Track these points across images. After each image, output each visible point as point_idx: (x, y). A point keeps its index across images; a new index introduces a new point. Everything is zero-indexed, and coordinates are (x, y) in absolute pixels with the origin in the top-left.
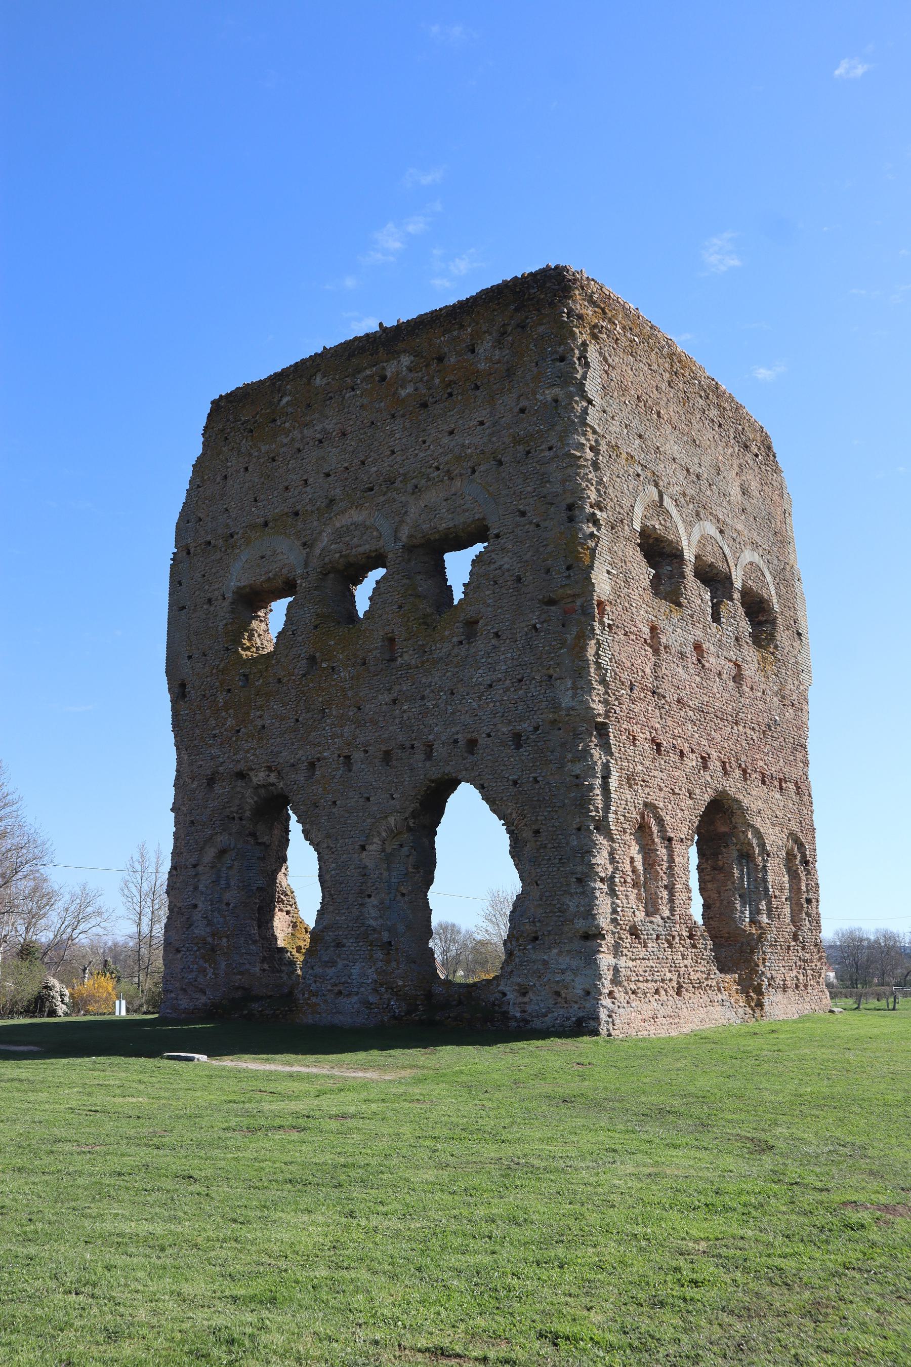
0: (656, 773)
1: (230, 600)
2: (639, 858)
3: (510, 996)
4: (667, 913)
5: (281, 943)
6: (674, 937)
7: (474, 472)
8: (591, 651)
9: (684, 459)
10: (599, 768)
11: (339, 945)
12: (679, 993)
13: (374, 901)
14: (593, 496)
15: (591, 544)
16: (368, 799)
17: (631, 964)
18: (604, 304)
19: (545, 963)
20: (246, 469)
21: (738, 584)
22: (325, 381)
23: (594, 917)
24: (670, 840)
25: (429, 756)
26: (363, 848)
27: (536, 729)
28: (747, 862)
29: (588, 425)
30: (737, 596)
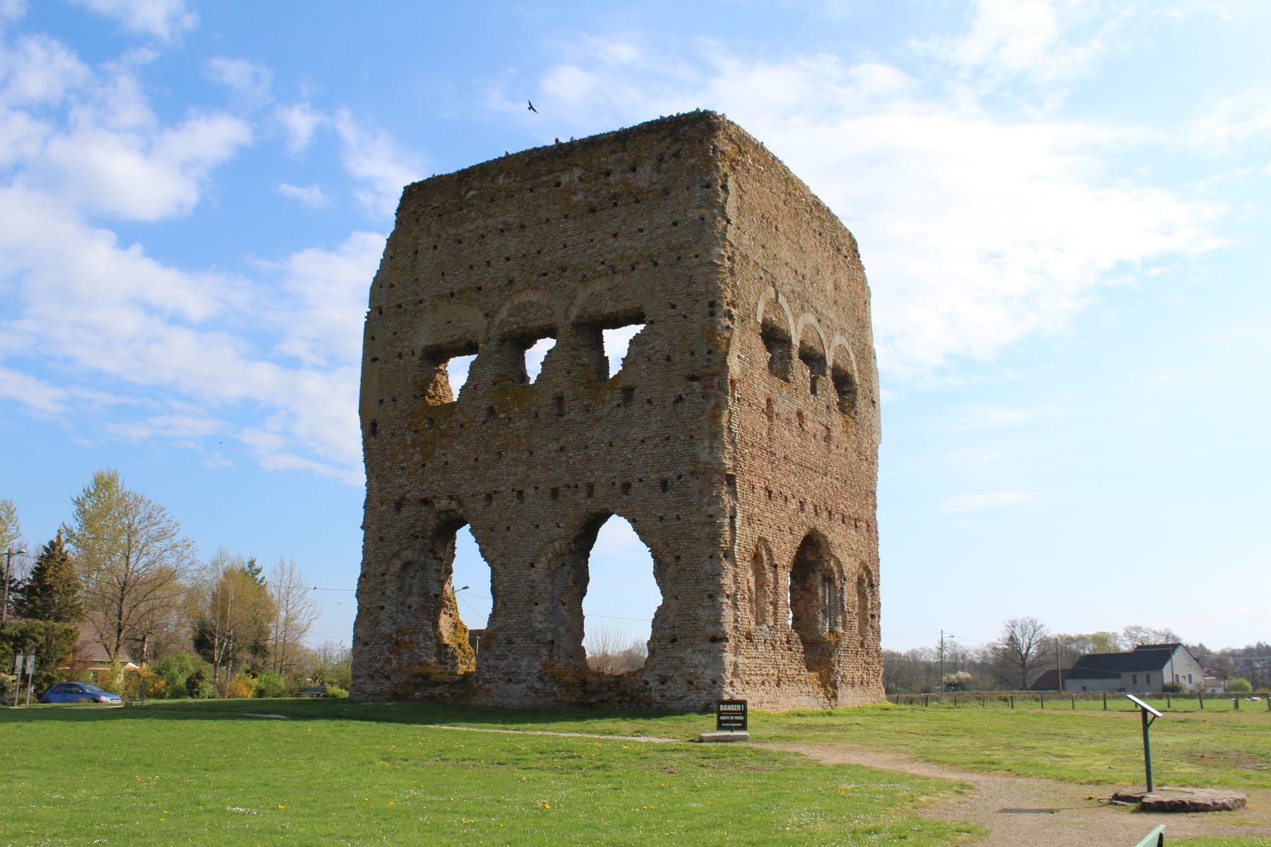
0: (767, 514)
2: (752, 579)
3: (653, 684)
4: (771, 623)
5: (446, 641)
7: (633, 269)
8: (725, 419)
9: (794, 263)
10: (728, 510)
11: (510, 642)
12: (778, 685)
13: (540, 608)
14: (729, 295)
15: (727, 334)
16: (537, 526)
17: (746, 661)
18: (743, 142)
19: (682, 660)
20: (435, 247)
21: (830, 363)
22: (507, 181)
23: (721, 624)
24: (776, 566)
25: (590, 494)
26: (532, 565)
27: (680, 477)
30: (829, 372)
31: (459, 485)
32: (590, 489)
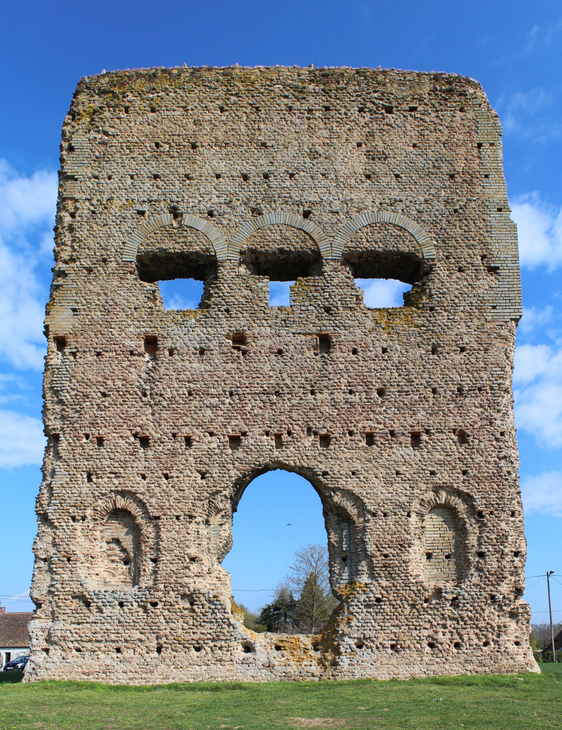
6: (154, 605)
9: (241, 167)
17: (72, 627)
28: (349, 526)
29: (67, 198)
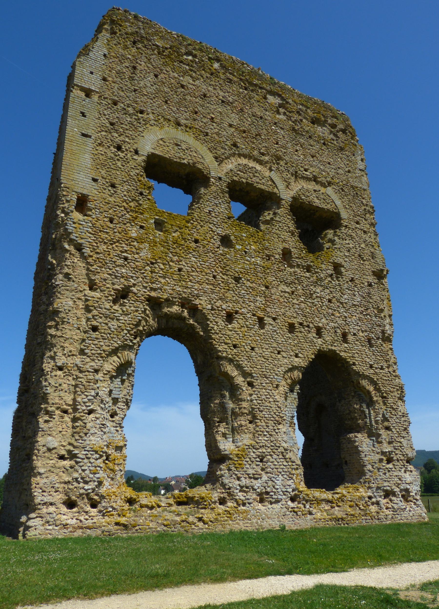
1: (144, 158)
31: (198, 296)
32: (319, 332)
